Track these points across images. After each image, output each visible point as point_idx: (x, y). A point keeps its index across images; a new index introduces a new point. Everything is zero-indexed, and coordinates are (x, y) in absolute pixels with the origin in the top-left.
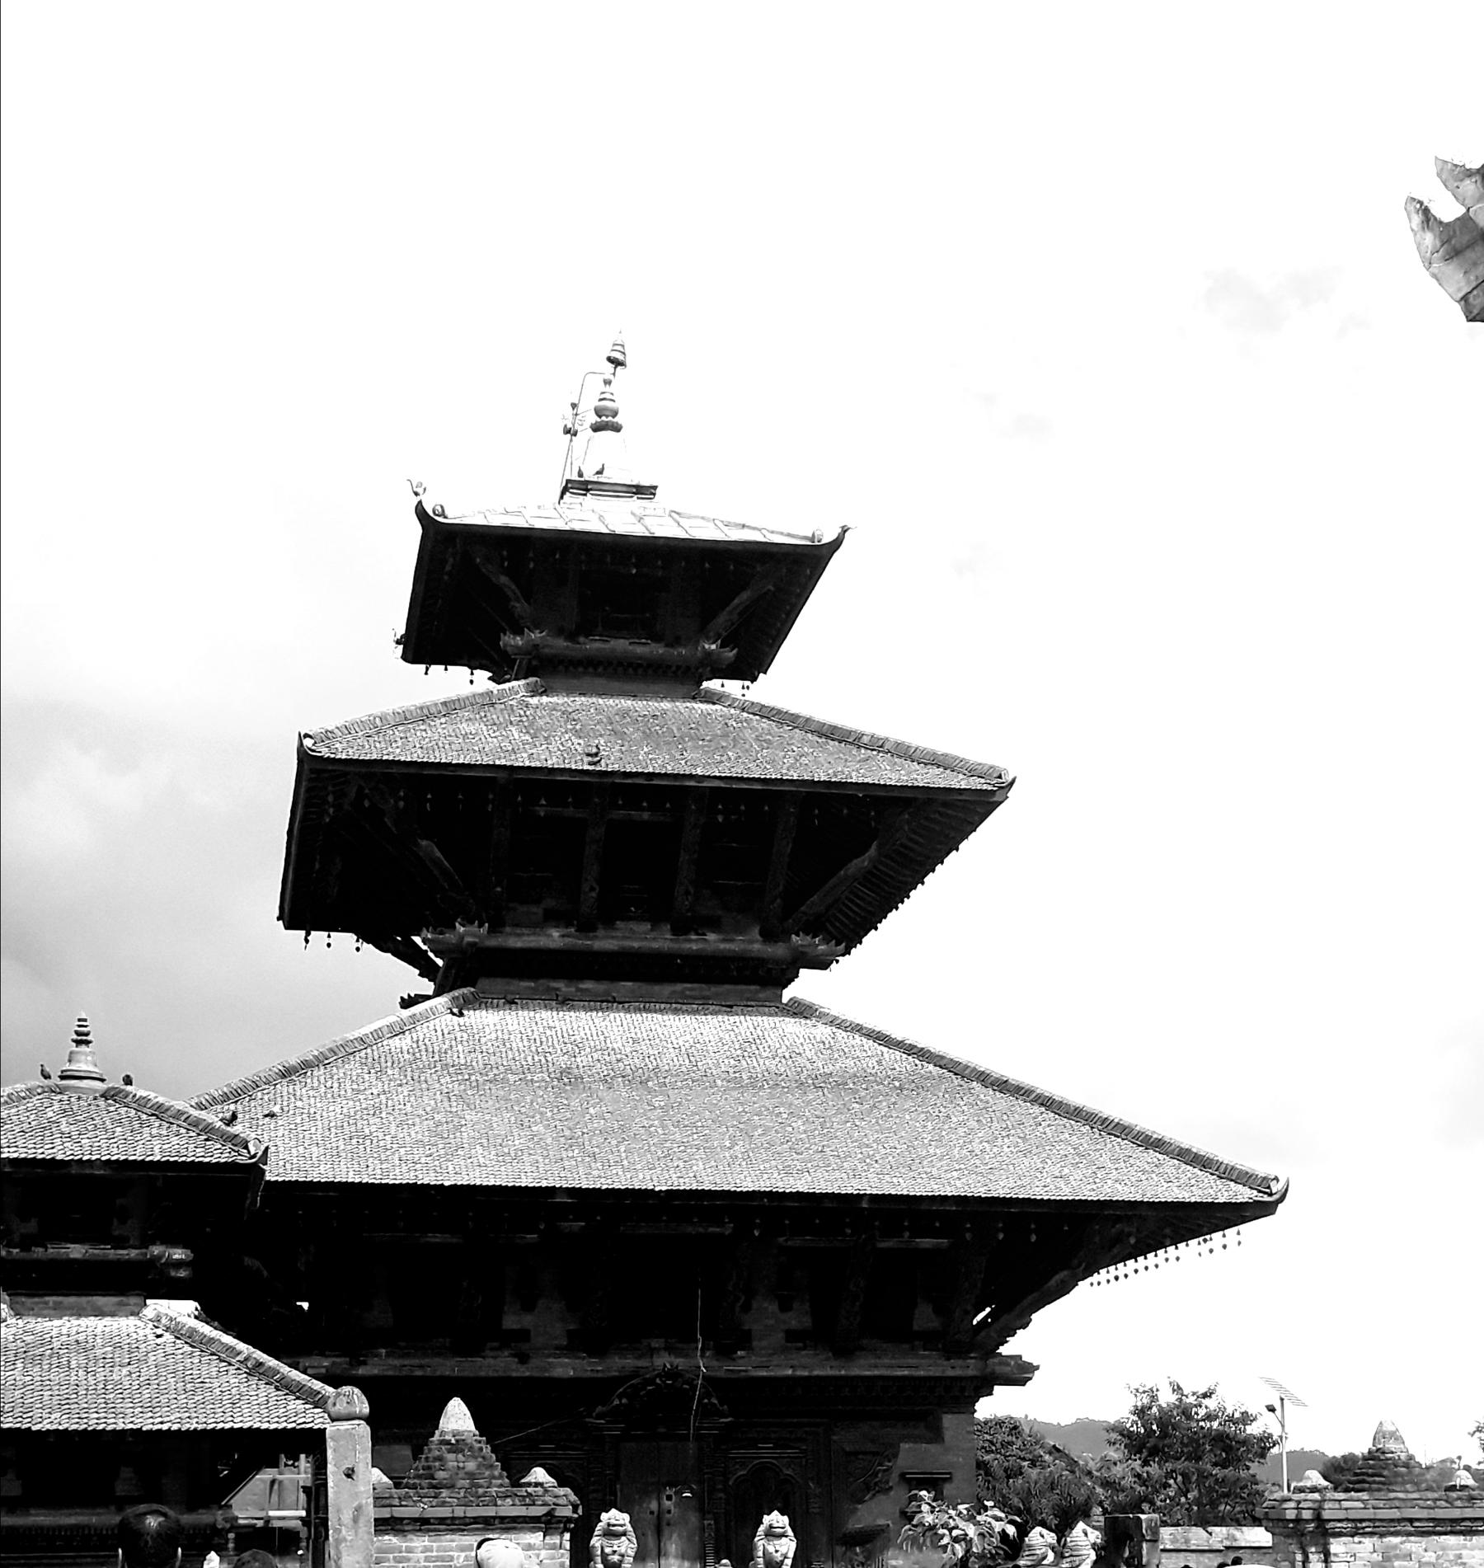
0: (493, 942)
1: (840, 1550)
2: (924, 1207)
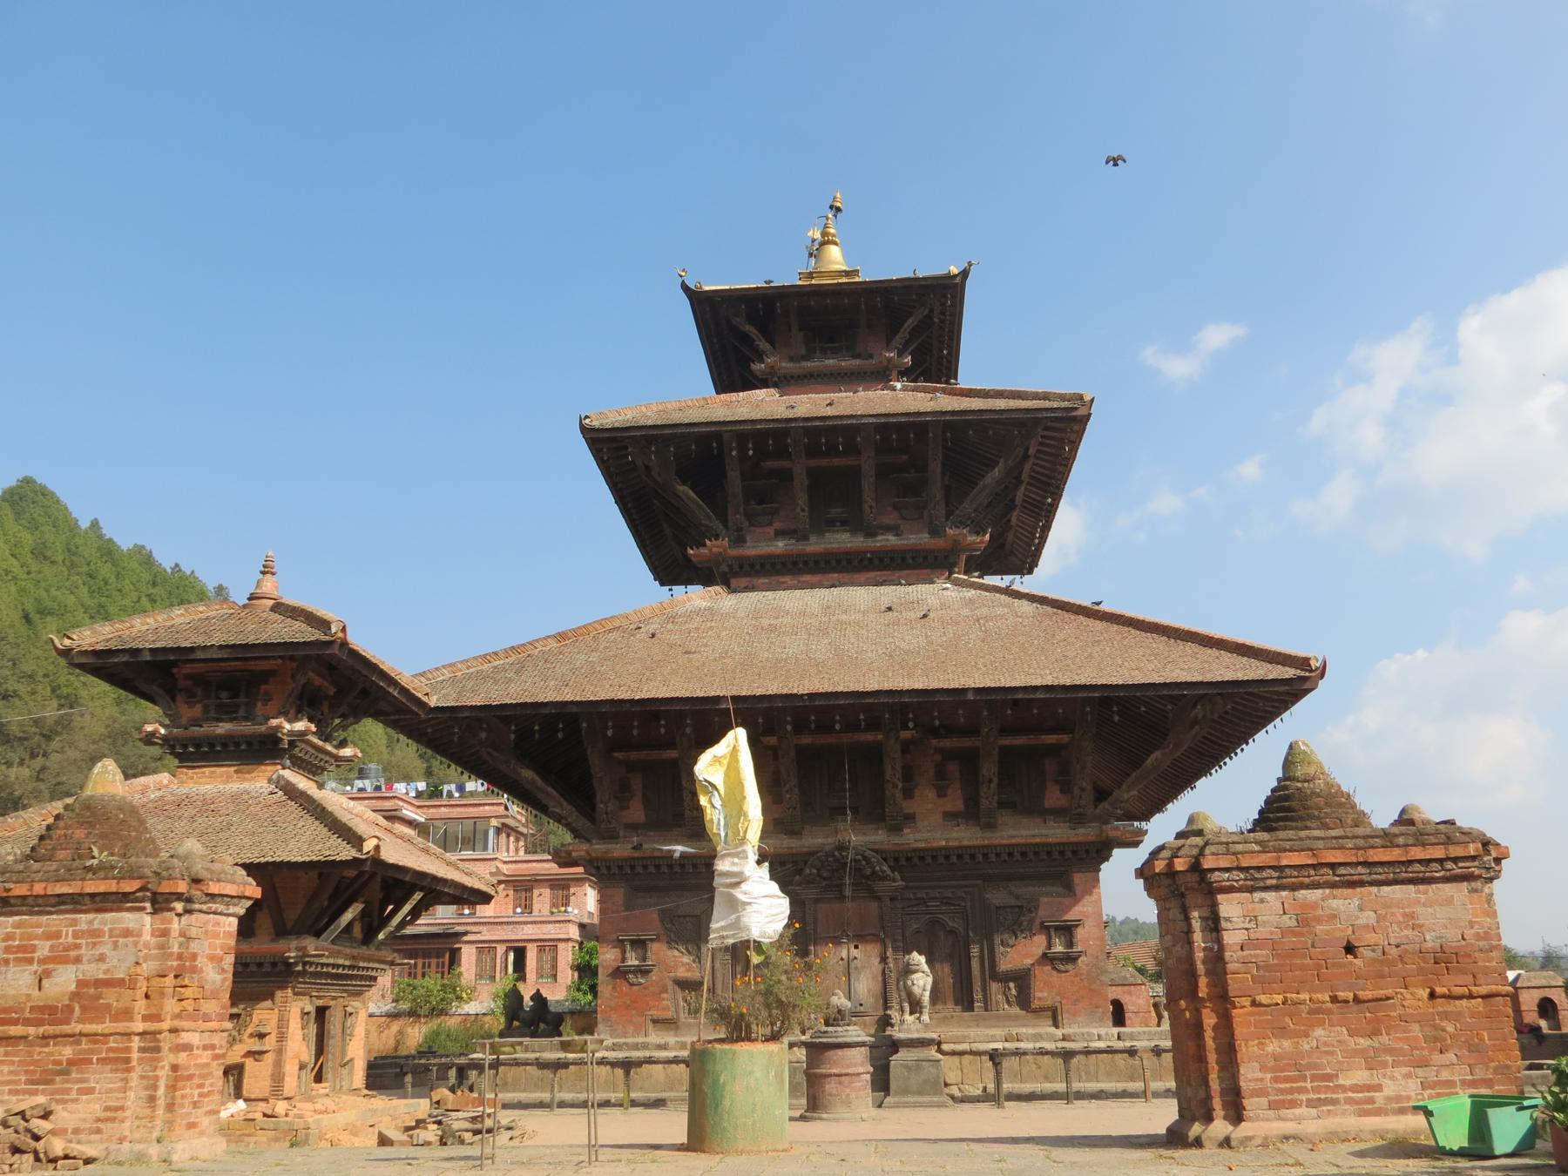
0: (735, 552)
1: (995, 987)
2: (1020, 696)
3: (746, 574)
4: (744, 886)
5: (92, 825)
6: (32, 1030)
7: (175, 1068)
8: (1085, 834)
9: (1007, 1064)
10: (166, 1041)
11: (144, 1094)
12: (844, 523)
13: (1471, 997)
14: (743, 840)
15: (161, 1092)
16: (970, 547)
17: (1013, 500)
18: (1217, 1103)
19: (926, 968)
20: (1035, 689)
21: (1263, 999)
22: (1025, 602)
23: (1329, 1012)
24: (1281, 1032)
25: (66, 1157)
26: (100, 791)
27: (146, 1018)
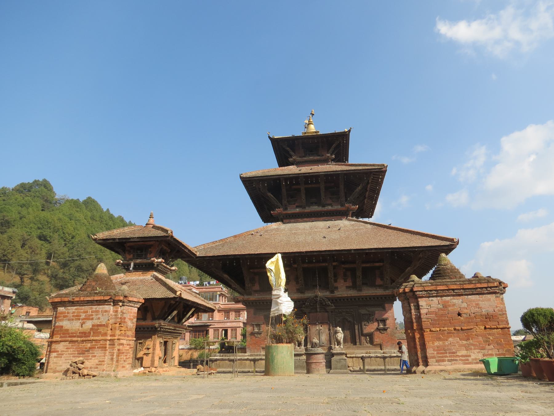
0: (285, 212)
1: (363, 338)
3: (288, 219)
4: (280, 298)
5: (97, 281)
6: (79, 339)
7: (119, 350)
8: (388, 292)
9: (367, 360)
10: (116, 342)
11: (110, 357)
12: (316, 203)
13: (497, 328)
14: (280, 285)
15: (115, 357)
16: (352, 210)
17: (365, 196)
18: (420, 361)
19: (341, 332)
20: (372, 249)
21: (433, 329)
22: (369, 225)
23: (453, 333)
24: (439, 339)
25: (88, 375)
26: (100, 272)
27: (111, 336)
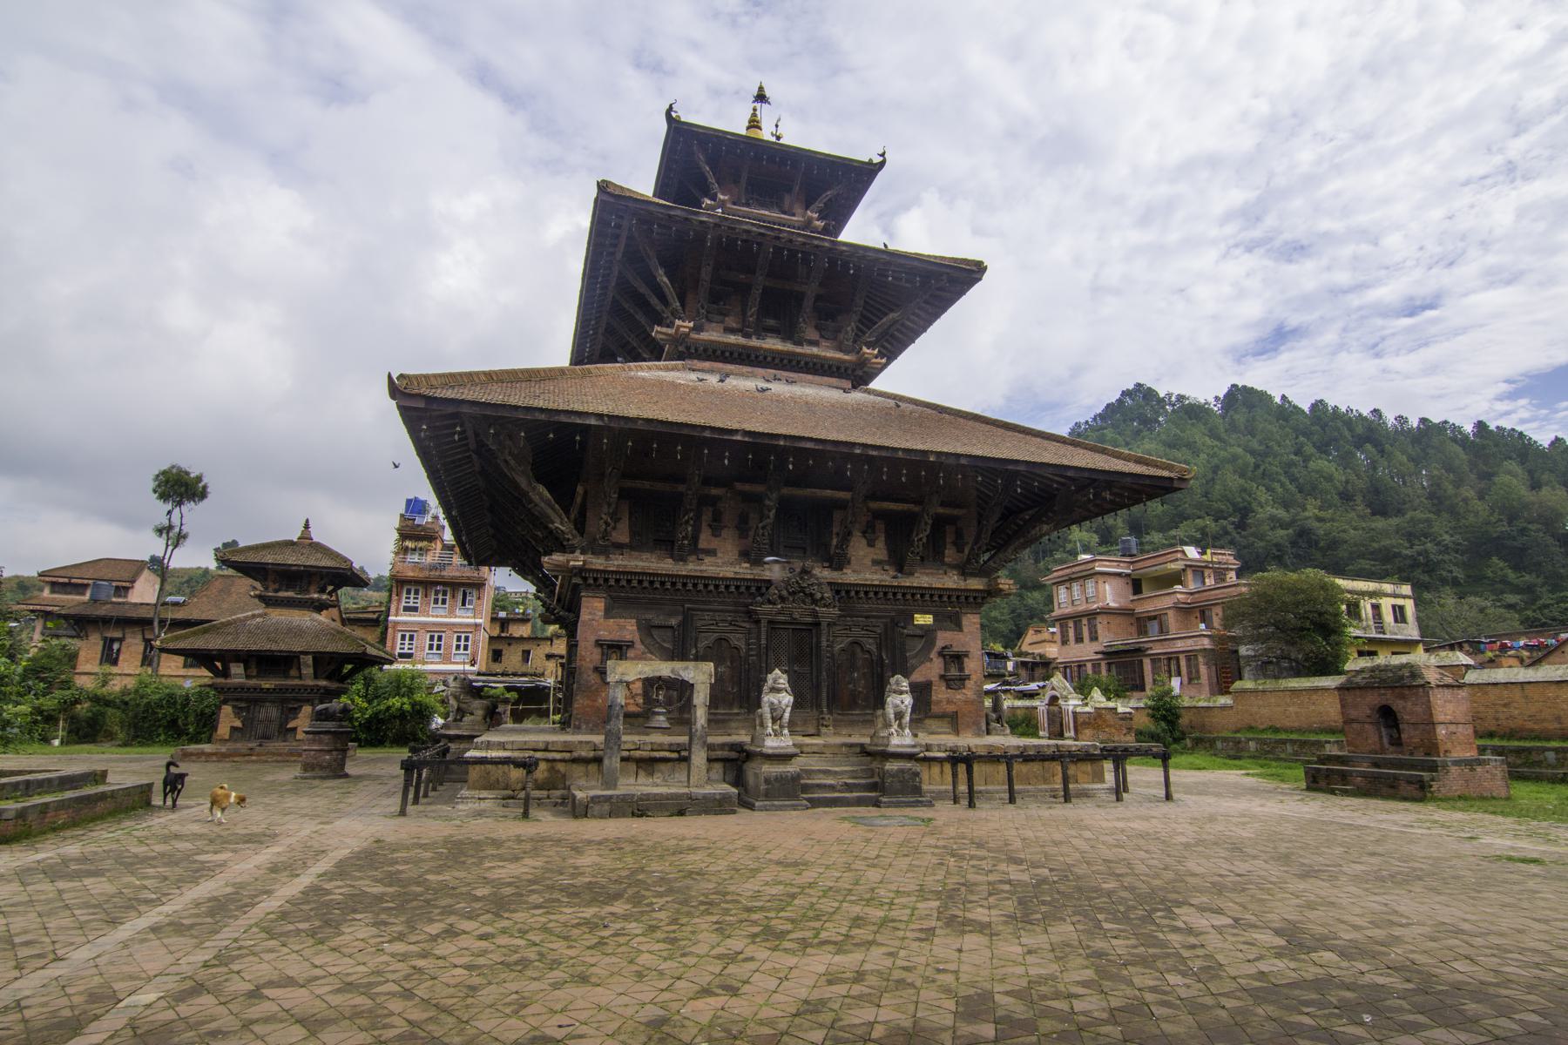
0: (694, 335)
8: (976, 584)
12: (775, 331)
